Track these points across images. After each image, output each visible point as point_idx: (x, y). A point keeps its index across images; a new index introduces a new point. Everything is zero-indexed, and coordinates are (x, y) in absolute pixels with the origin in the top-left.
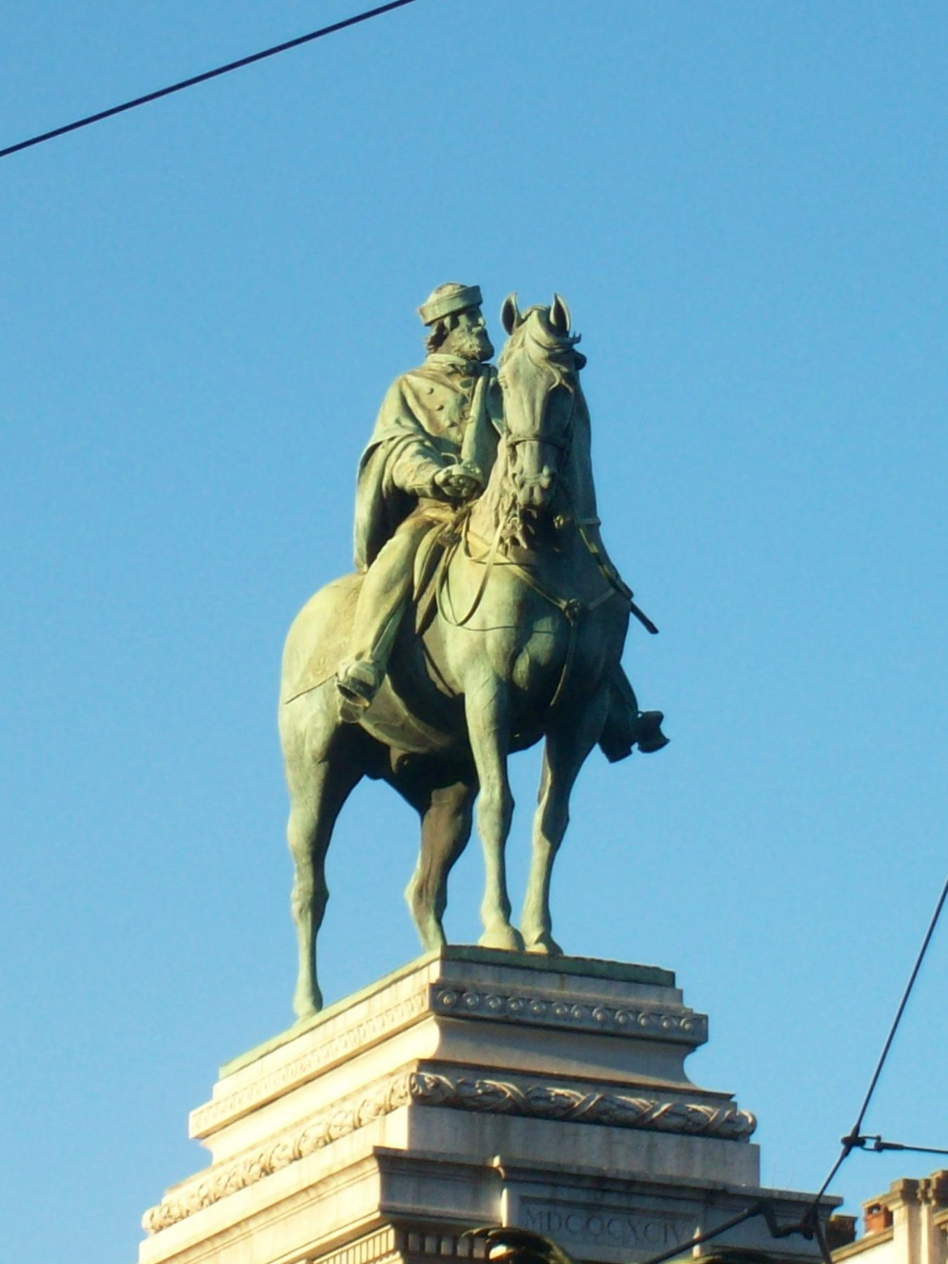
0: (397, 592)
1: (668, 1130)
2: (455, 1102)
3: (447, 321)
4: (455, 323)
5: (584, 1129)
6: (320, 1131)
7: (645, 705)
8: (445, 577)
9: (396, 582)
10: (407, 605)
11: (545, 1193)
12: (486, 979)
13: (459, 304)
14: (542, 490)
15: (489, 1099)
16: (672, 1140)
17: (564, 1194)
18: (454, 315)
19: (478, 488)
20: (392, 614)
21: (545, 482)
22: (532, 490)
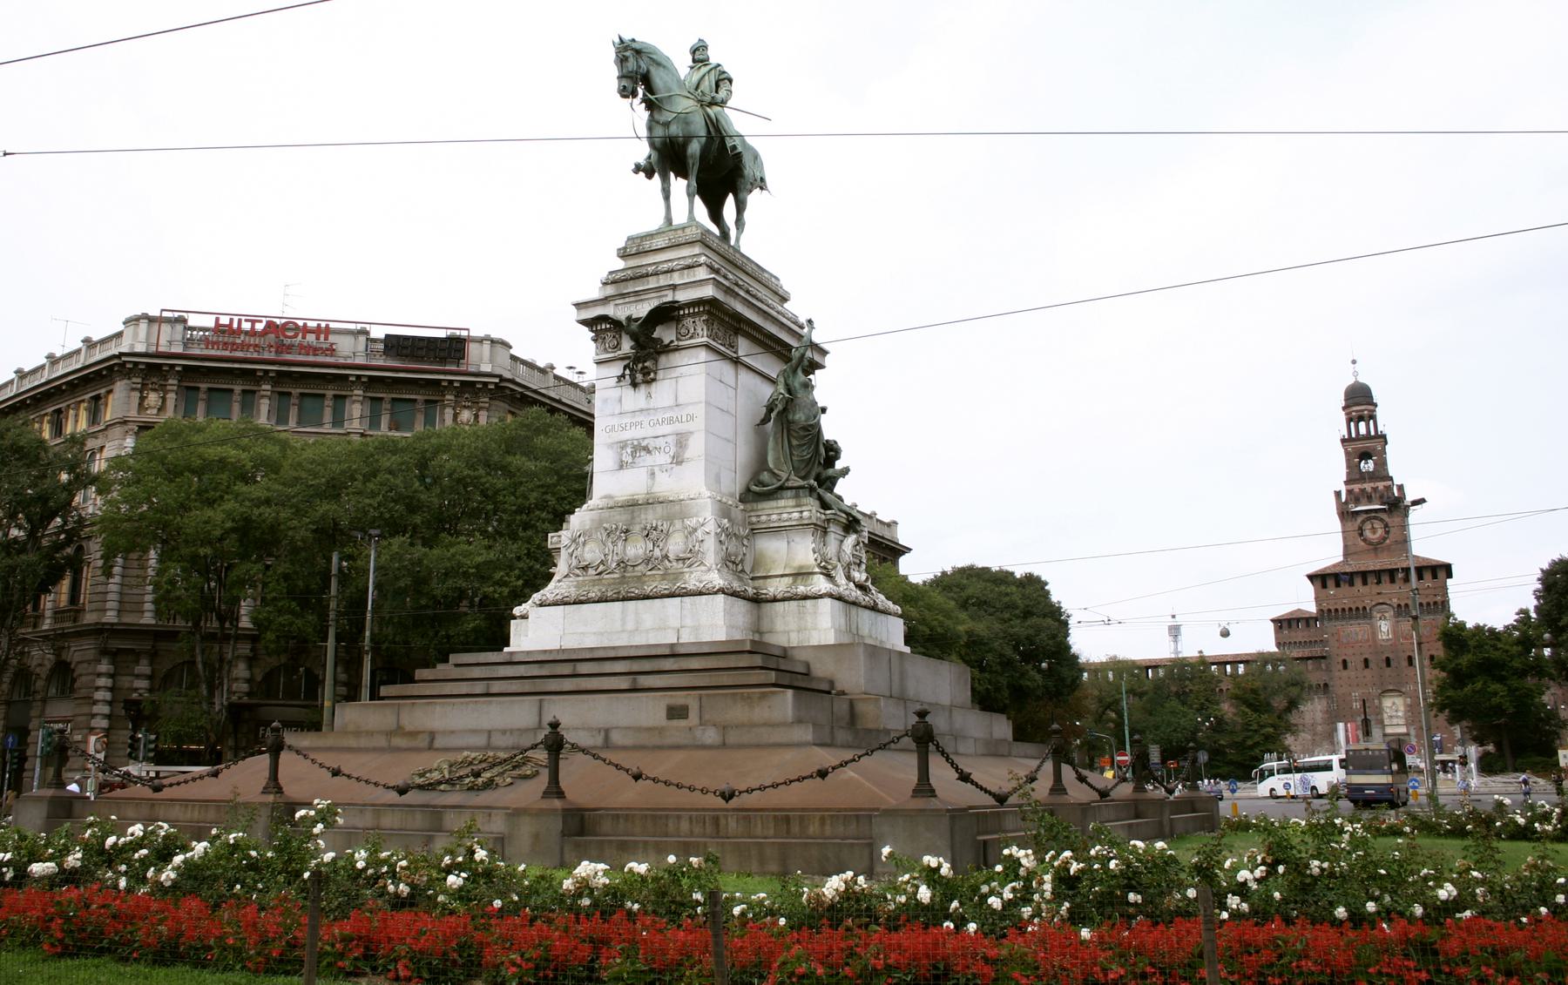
2: (614, 282)
5: (650, 278)
17: (627, 300)
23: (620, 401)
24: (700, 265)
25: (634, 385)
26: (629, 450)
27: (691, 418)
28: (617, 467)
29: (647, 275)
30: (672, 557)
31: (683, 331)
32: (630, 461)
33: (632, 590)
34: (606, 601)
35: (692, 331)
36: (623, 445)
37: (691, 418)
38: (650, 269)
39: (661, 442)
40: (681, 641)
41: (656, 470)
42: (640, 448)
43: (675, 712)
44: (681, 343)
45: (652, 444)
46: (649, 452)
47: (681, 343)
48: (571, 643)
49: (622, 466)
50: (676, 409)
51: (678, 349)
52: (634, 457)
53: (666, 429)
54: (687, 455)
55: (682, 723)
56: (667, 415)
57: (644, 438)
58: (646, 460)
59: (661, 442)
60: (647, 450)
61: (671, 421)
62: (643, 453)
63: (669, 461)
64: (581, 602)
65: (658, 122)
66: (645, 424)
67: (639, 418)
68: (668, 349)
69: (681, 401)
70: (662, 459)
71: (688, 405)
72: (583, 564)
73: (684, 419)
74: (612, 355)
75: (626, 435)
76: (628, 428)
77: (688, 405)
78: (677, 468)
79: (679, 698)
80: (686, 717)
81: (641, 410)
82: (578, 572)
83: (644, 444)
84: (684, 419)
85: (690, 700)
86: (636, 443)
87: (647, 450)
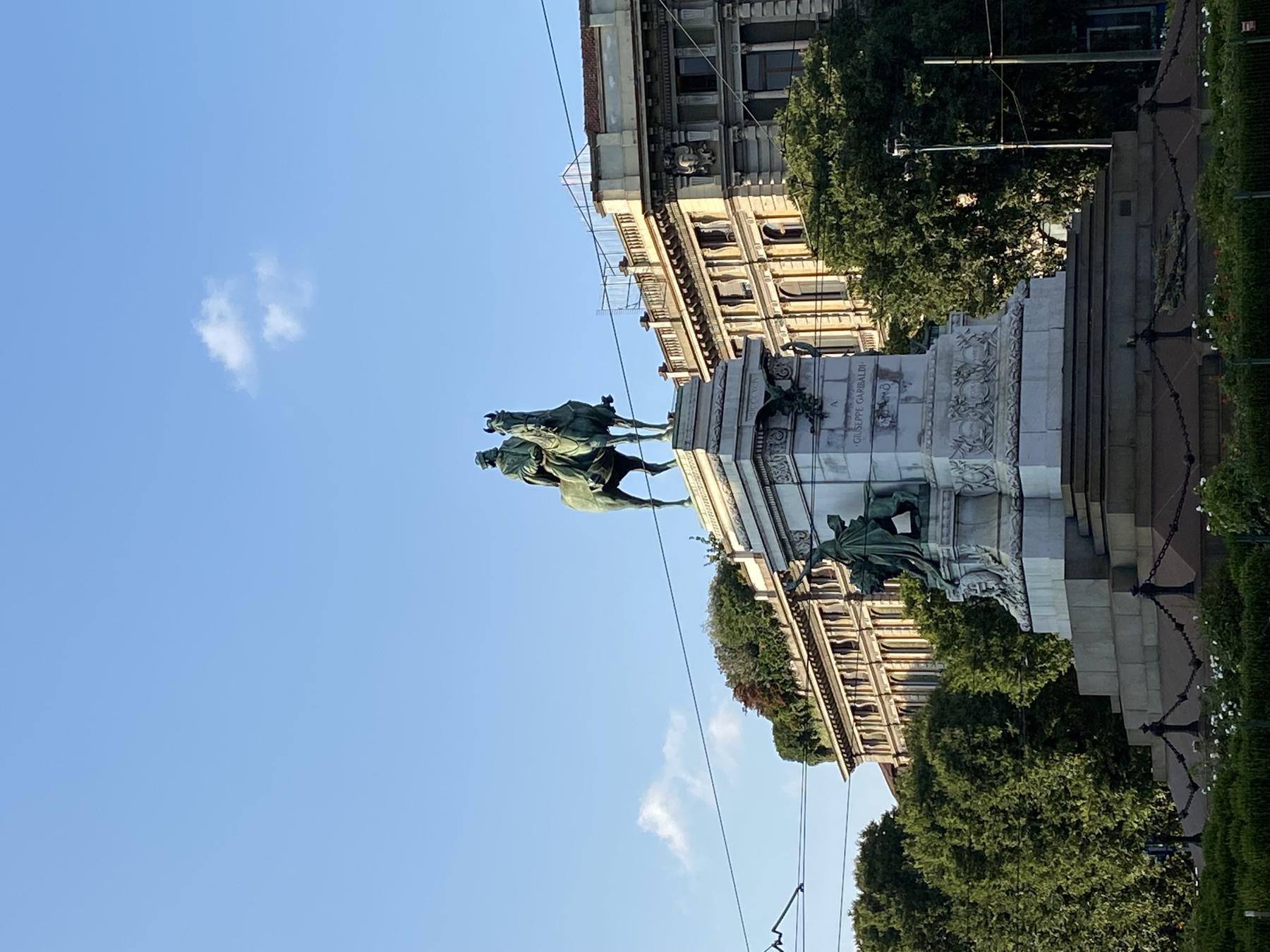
0: (568, 469)
7: (600, 402)
8: (563, 454)
10: (570, 466)
19: (538, 448)
23: (832, 430)
24: (727, 367)
25: (822, 416)
26: (881, 420)
27: (862, 368)
28: (894, 432)
30: (985, 359)
31: (785, 373)
32: (890, 419)
33: (1012, 375)
35: (786, 367)
36: (874, 425)
37: (862, 368)
38: (717, 407)
39: (879, 392)
40: (1062, 326)
41: (903, 396)
42: (878, 412)
43: (1125, 210)
45: (879, 400)
46: (885, 403)
48: (1056, 420)
49: (894, 426)
50: (852, 379)
52: (888, 416)
53: (868, 388)
54: (894, 369)
55: (1133, 205)
57: (873, 407)
58: (892, 403)
60: (882, 406)
61: (862, 385)
62: (886, 408)
63: (897, 385)
64: (1018, 421)
65: (571, 422)
66: (859, 406)
67: (853, 411)
68: (795, 384)
69: (845, 376)
71: (850, 370)
72: (981, 436)
73: (863, 373)
74: (789, 438)
75: (866, 423)
76: (857, 422)
77: (850, 370)
78: (905, 379)
79: (1115, 207)
80: (1129, 202)
81: (847, 410)
82: (988, 440)
83: (877, 407)
84: (863, 373)
85: (1117, 198)
87: (882, 406)
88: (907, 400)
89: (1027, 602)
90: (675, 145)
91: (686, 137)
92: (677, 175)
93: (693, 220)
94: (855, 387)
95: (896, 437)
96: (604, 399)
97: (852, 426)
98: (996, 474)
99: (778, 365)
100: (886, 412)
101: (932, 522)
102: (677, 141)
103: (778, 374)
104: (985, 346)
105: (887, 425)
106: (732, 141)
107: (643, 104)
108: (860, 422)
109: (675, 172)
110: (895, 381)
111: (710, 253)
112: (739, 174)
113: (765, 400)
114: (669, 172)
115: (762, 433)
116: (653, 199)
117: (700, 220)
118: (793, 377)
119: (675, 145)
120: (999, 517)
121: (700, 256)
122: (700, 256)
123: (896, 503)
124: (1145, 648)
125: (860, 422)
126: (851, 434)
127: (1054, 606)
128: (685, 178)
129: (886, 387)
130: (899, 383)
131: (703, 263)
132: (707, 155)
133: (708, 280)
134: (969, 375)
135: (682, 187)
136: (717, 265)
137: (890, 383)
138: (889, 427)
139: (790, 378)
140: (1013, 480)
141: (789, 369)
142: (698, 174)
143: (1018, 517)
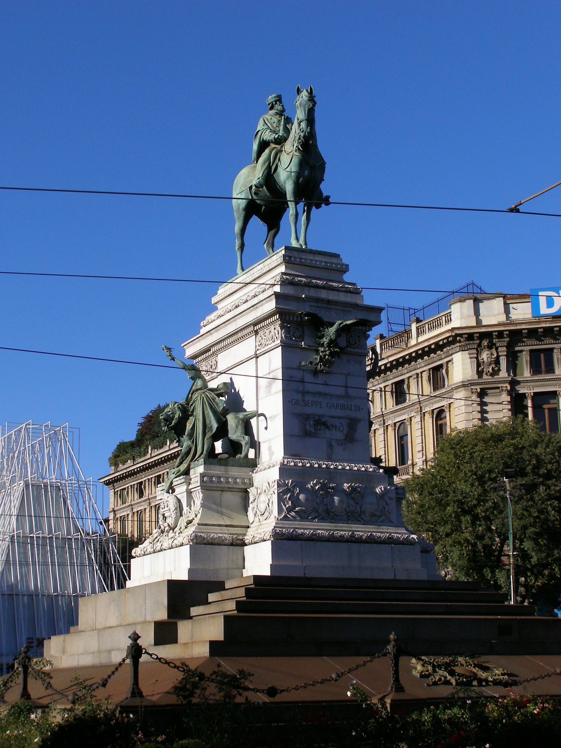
0: (267, 164)
1: (342, 291)
3: (274, 103)
4: (276, 103)
5: (322, 290)
6: (253, 294)
7: (325, 194)
8: (279, 160)
9: (266, 162)
10: (269, 167)
11: (315, 304)
12: (295, 254)
13: (277, 99)
14: (308, 133)
15: (299, 282)
16: (343, 293)
17: (320, 305)
18: (276, 101)
19: (285, 139)
20: (265, 170)
21: (309, 130)
22: (305, 132)
26: (312, 423)
29: (317, 287)
32: (313, 431)
34: (335, 541)
40: (397, 578)
41: (334, 443)
44: (352, 350)
45: (330, 421)
46: (327, 427)
47: (352, 350)
49: (307, 434)
51: (351, 354)
52: (316, 429)
56: (341, 402)
57: (323, 416)
59: (336, 422)
60: (325, 424)
62: (323, 427)
63: (343, 437)
70: (339, 435)
73: (353, 408)
81: (320, 394)
83: (324, 420)
84: (353, 408)
86: (317, 418)
87: (325, 425)
88: (330, 446)
89: (154, 552)
90: (497, 349)
91: (502, 355)
92: (477, 350)
93: (447, 362)
94: (341, 402)
95: (297, 436)
96: (328, 197)
97: (307, 398)
98: (265, 522)
99: (359, 337)
100: (319, 427)
101: (223, 468)
102: (500, 349)
103: (351, 336)
104: (378, 513)
105: (308, 428)
106: (500, 385)
107: (524, 327)
108: (310, 404)
109: (479, 350)
110: (346, 436)
111: (425, 375)
112: (479, 390)
113: (327, 322)
114: (479, 345)
115: (299, 319)
116: (461, 335)
117: (447, 367)
118: (349, 349)
119: (497, 349)
120: (226, 526)
121: (424, 369)
122: (424, 369)
123: (239, 438)
124: (109, 651)
125: (310, 404)
126: (299, 397)
127: (151, 575)
128: (476, 356)
129: (341, 429)
130: (345, 439)
131: (418, 371)
132: (490, 370)
133: (408, 375)
134: (353, 499)
135: (469, 354)
136: (418, 381)
137: (345, 432)
138: (306, 430)
139: (347, 346)
140: (259, 536)
141: (356, 346)
142: (478, 365)
143: (226, 542)
